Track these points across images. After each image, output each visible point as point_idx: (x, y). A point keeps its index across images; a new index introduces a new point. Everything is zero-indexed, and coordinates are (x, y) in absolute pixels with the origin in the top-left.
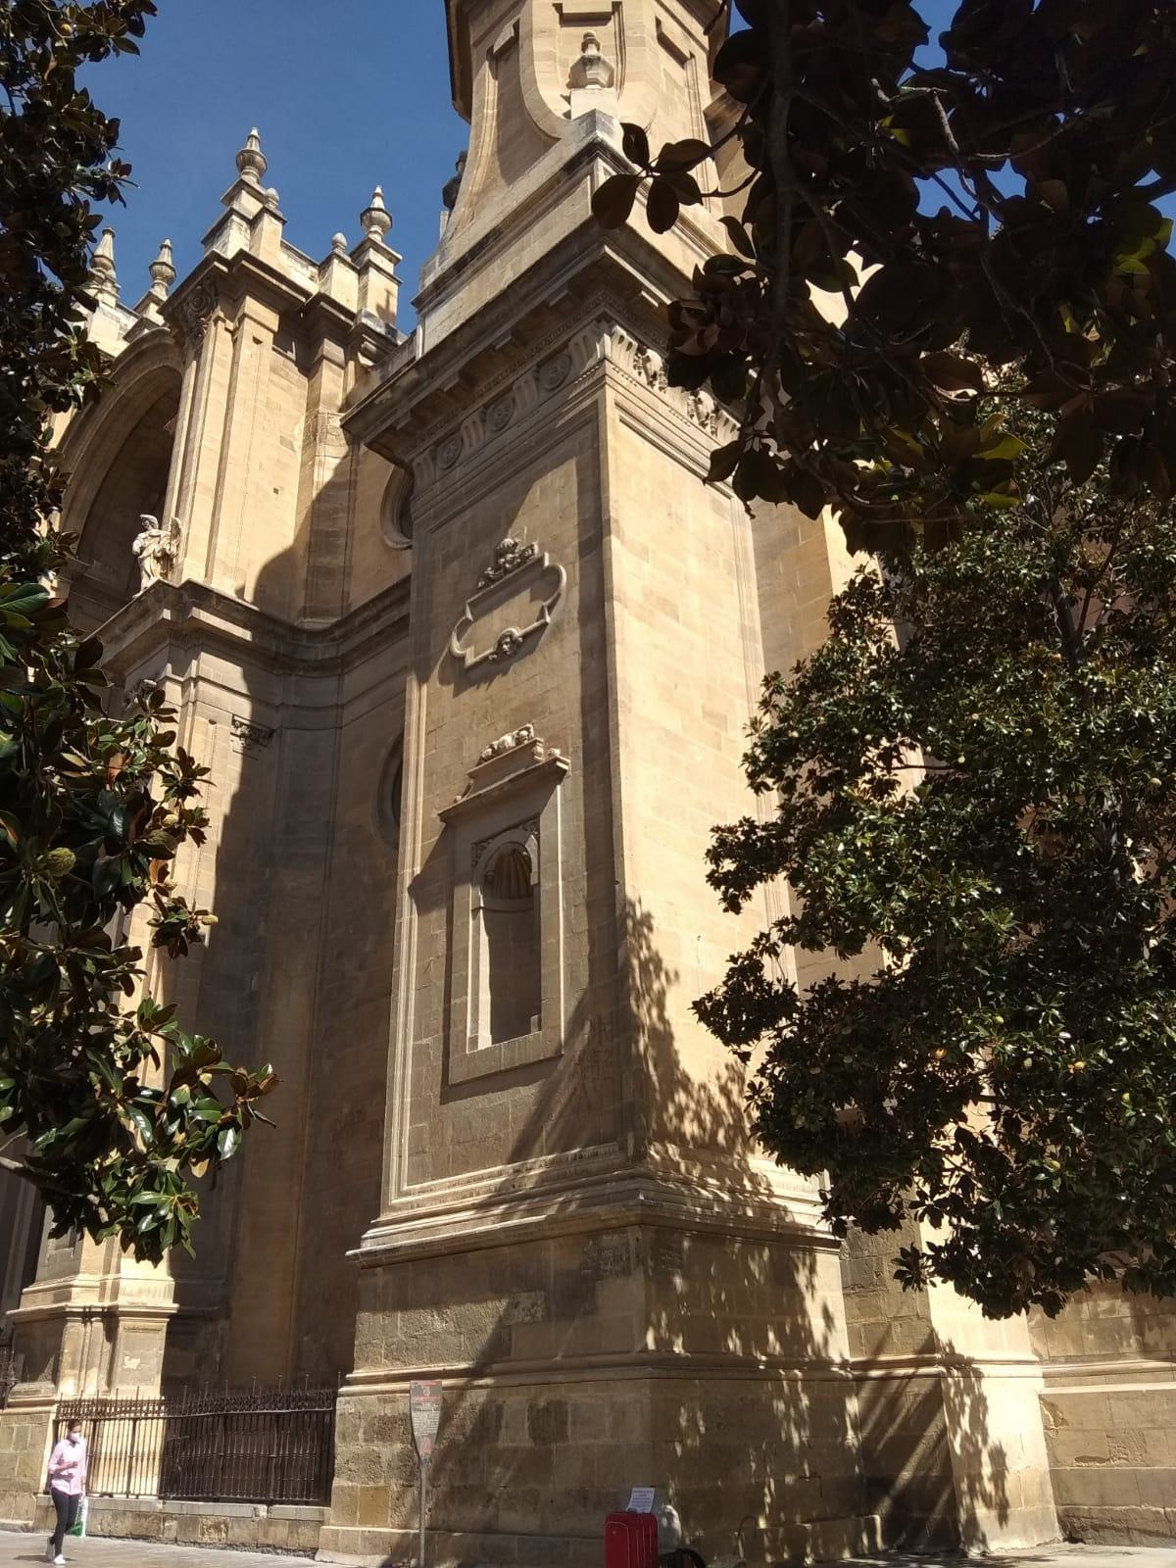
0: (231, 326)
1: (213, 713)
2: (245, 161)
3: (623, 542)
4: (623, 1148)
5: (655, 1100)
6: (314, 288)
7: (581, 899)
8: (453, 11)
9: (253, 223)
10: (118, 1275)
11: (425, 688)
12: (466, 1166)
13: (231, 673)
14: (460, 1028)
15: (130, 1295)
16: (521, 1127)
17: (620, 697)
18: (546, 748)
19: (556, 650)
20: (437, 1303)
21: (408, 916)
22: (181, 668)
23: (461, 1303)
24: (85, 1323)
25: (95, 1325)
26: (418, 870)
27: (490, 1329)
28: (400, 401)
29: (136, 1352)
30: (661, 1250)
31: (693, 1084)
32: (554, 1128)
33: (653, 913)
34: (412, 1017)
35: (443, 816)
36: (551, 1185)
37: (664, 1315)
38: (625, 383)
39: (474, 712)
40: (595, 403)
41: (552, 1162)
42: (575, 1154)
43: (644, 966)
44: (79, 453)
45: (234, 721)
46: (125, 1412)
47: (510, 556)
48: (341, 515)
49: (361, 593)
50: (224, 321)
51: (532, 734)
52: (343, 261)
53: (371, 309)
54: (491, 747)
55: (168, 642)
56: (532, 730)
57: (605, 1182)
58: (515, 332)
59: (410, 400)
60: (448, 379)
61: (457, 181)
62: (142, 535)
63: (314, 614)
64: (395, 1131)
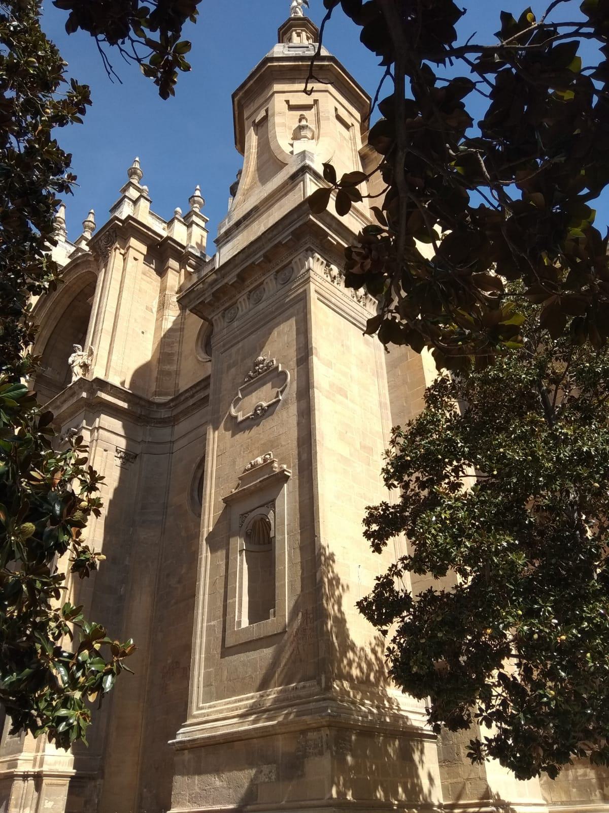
0: (123, 251)
1: (106, 445)
2: (133, 173)
3: (319, 359)
4: (319, 683)
6: (165, 234)
7: (297, 545)
8: (236, 103)
9: (135, 202)
10: (43, 754)
11: (217, 433)
12: (234, 693)
13: (116, 425)
14: (232, 616)
16: (264, 671)
17: (318, 438)
18: (279, 464)
19: (284, 413)
20: (217, 771)
21: (205, 553)
22: (90, 422)
23: (230, 771)
24: (24, 781)
25: (30, 782)
26: (211, 529)
27: (246, 785)
28: (207, 289)
29: (51, 798)
30: (340, 741)
31: (357, 648)
32: (282, 672)
33: (335, 553)
34: (206, 610)
35: (225, 500)
36: (280, 704)
37: (341, 778)
38: (320, 281)
39: (242, 446)
40: (305, 290)
41: (281, 691)
42: (293, 687)
43: (330, 582)
44: (43, 314)
45: (117, 450)
47: (261, 365)
48: (175, 344)
49: (185, 384)
50: (119, 250)
51: (272, 457)
52: (180, 221)
53: (193, 244)
54: (251, 463)
55: (85, 408)
56: (272, 455)
57: (309, 702)
59: (212, 289)
60: (231, 278)
61: (237, 183)
62: (74, 355)
63: (160, 395)
64: (196, 673)
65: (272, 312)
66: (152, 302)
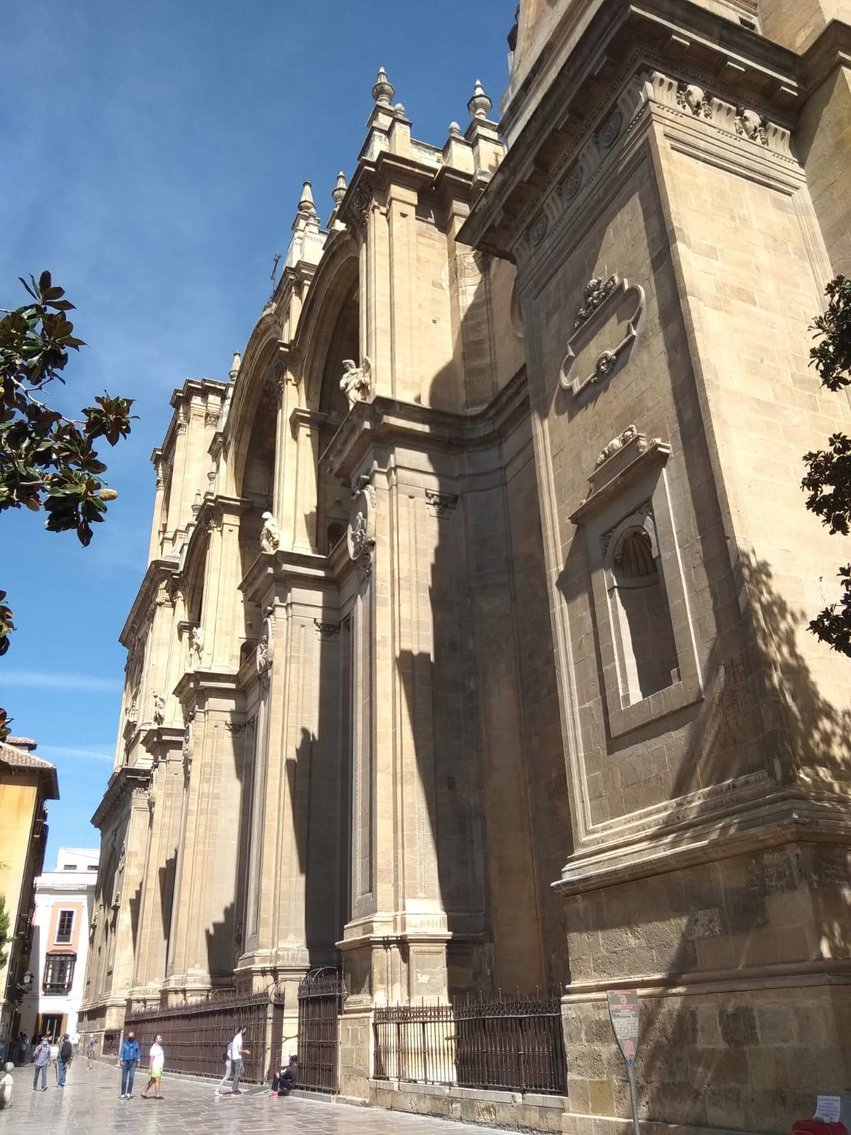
0: (384, 210)
1: (411, 490)
2: (379, 91)
3: (689, 246)
4: (772, 774)
5: (798, 728)
6: (439, 167)
7: (698, 561)
9: (388, 133)
10: (404, 912)
11: (546, 422)
12: (637, 805)
13: (419, 459)
14: (614, 689)
15: (415, 926)
16: (677, 766)
17: (706, 376)
18: (648, 441)
19: (645, 357)
20: (628, 922)
21: (559, 606)
22: (383, 462)
23: (649, 921)
24: (386, 948)
25: (393, 949)
26: (561, 568)
27: (676, 943)
28: (494, 203)
29: (425, 970)
30: (824, 864)
31: (836, 712)
32: (706, 763)
33: (769, 561)
34: (575, 687)
35: (575, 519)
36: (709, 815)
37: (836, 925)
38: (671, 116)
39: (586, 429)
40: (647, 139)
41: (709, 794)
42: (729, 785)
43: (767, 609)
44: (308, 339)
45: (427, 494)
46: (417, 1017)
47: (596, 293)
48: (483, 326)
49: (503, 379)
50: (379, 208)
51: (635, 432)
52: (459, 141)
53: (485, 168)
54: (604, 453)
55: (371, 446)
56: (634, 429)
57: (758, 806)
58: (571, 110)
59: (501, 200)
61: (516, 27)
62: (345, 375)
63: (474, 404)
64: (576, 781)
65: (600, 200)
66: (440, 274)
